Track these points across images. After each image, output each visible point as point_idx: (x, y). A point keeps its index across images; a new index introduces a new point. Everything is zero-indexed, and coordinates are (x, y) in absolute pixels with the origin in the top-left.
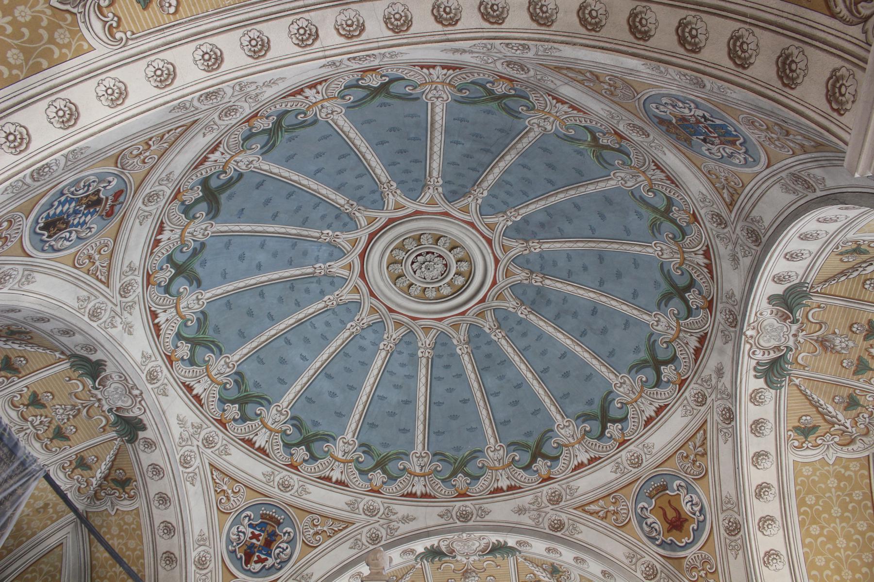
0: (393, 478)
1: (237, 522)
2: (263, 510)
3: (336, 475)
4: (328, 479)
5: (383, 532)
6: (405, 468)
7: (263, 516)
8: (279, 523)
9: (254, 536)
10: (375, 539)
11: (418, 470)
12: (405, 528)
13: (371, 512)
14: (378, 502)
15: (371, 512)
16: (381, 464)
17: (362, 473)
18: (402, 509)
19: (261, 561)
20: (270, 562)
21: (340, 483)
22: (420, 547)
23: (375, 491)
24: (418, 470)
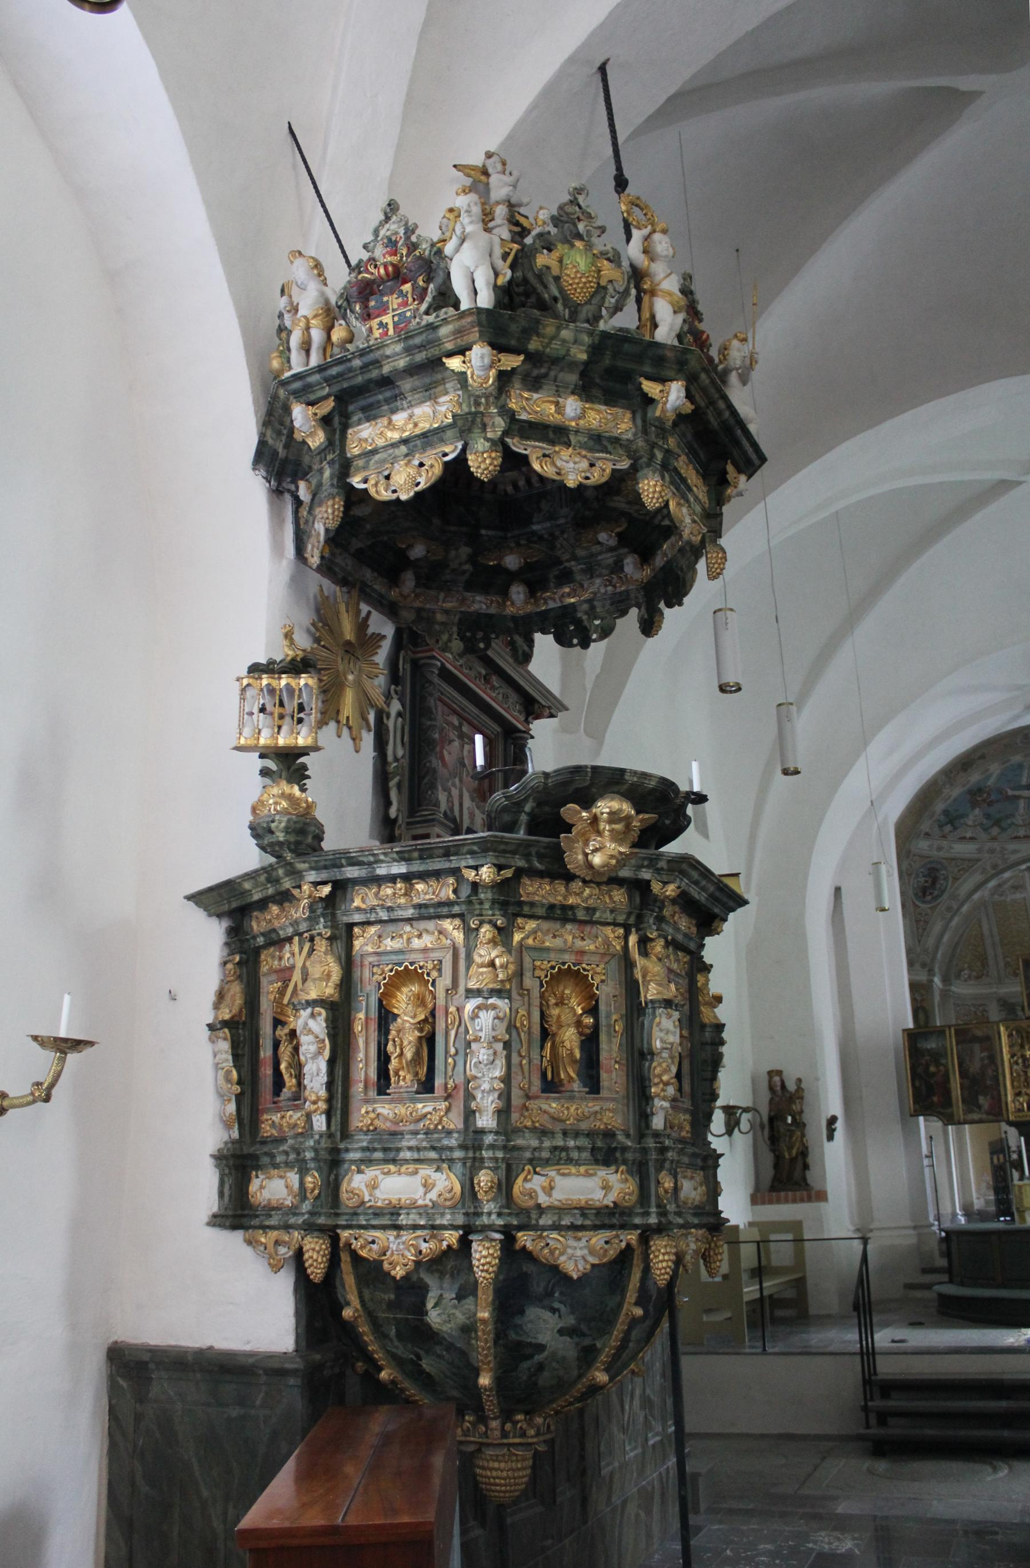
0: (1004, 830)
1: (917, 876)
2: (929, 866)
3: (968, 835)
4: (964, 838)
5: (1000, 862)
6: (1013, 823)
7: (929, 869)
8: (937, 870)
9: (926, 882)
10: (995, 866)
11: (1021, 822)
12: (1013, 858)
13: (992, 851)
14: (996, 845)
15: (992, 851)
16: (997, 823)
17: (985, 830)
18: (1011, 846)
19: (931, 894)
20: (936, 893)
21: (972, 839)
22: (1024, 867)
23: (994, 839)
24: (1021, 822)
